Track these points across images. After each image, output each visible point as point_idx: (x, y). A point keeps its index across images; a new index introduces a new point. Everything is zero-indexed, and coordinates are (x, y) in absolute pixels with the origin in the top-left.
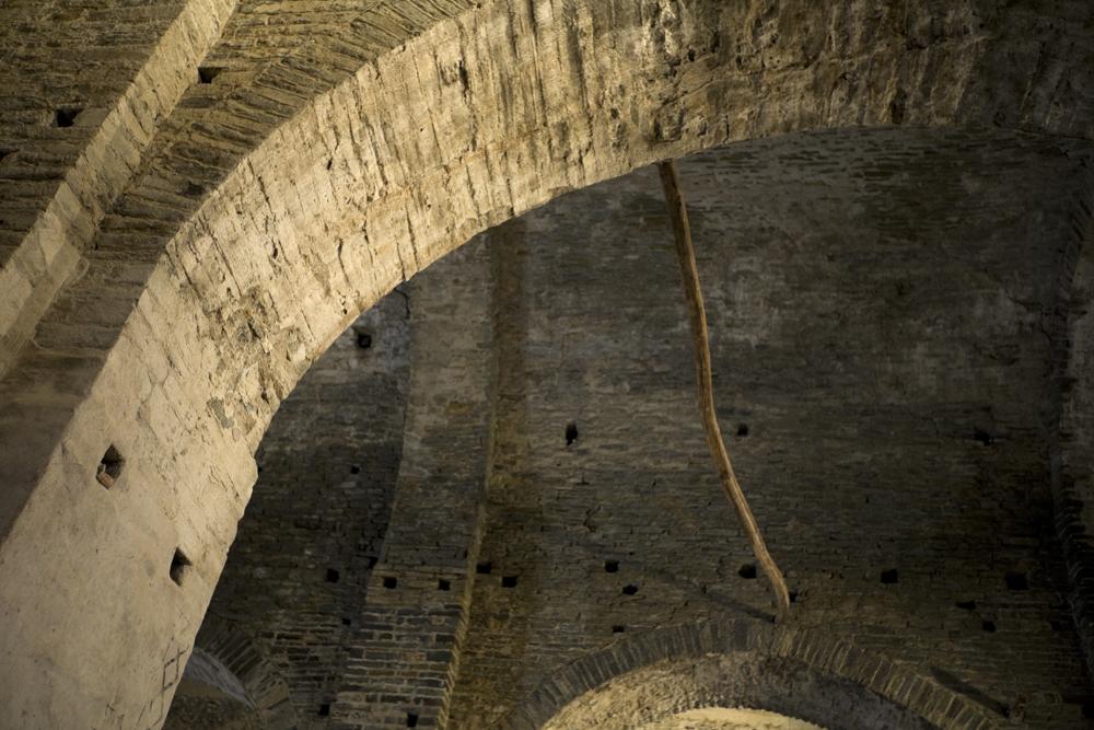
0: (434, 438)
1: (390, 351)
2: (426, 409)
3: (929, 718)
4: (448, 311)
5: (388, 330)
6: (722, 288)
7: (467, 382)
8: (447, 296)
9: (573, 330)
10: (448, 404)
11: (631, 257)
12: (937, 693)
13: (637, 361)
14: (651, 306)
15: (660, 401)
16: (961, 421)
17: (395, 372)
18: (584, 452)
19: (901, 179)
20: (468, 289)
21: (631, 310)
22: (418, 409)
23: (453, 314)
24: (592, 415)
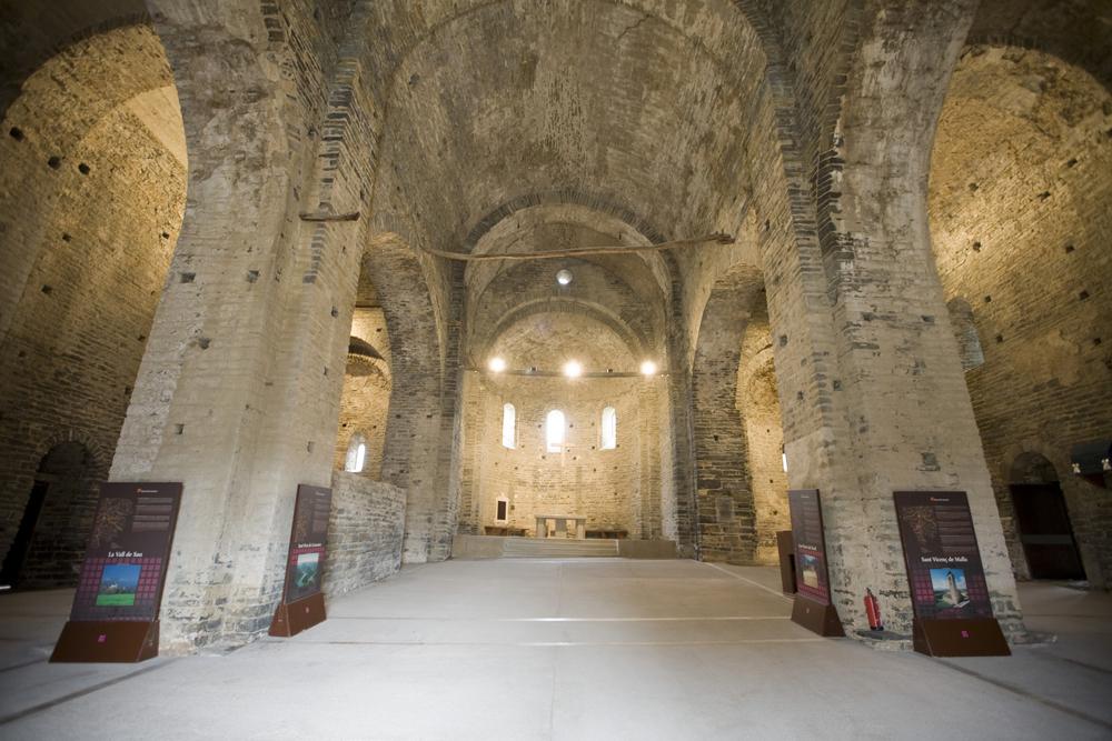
13: (455, 88)
14: (483, 81)
18: (410, 96)
19: (546, 149)
21: (479, 73)
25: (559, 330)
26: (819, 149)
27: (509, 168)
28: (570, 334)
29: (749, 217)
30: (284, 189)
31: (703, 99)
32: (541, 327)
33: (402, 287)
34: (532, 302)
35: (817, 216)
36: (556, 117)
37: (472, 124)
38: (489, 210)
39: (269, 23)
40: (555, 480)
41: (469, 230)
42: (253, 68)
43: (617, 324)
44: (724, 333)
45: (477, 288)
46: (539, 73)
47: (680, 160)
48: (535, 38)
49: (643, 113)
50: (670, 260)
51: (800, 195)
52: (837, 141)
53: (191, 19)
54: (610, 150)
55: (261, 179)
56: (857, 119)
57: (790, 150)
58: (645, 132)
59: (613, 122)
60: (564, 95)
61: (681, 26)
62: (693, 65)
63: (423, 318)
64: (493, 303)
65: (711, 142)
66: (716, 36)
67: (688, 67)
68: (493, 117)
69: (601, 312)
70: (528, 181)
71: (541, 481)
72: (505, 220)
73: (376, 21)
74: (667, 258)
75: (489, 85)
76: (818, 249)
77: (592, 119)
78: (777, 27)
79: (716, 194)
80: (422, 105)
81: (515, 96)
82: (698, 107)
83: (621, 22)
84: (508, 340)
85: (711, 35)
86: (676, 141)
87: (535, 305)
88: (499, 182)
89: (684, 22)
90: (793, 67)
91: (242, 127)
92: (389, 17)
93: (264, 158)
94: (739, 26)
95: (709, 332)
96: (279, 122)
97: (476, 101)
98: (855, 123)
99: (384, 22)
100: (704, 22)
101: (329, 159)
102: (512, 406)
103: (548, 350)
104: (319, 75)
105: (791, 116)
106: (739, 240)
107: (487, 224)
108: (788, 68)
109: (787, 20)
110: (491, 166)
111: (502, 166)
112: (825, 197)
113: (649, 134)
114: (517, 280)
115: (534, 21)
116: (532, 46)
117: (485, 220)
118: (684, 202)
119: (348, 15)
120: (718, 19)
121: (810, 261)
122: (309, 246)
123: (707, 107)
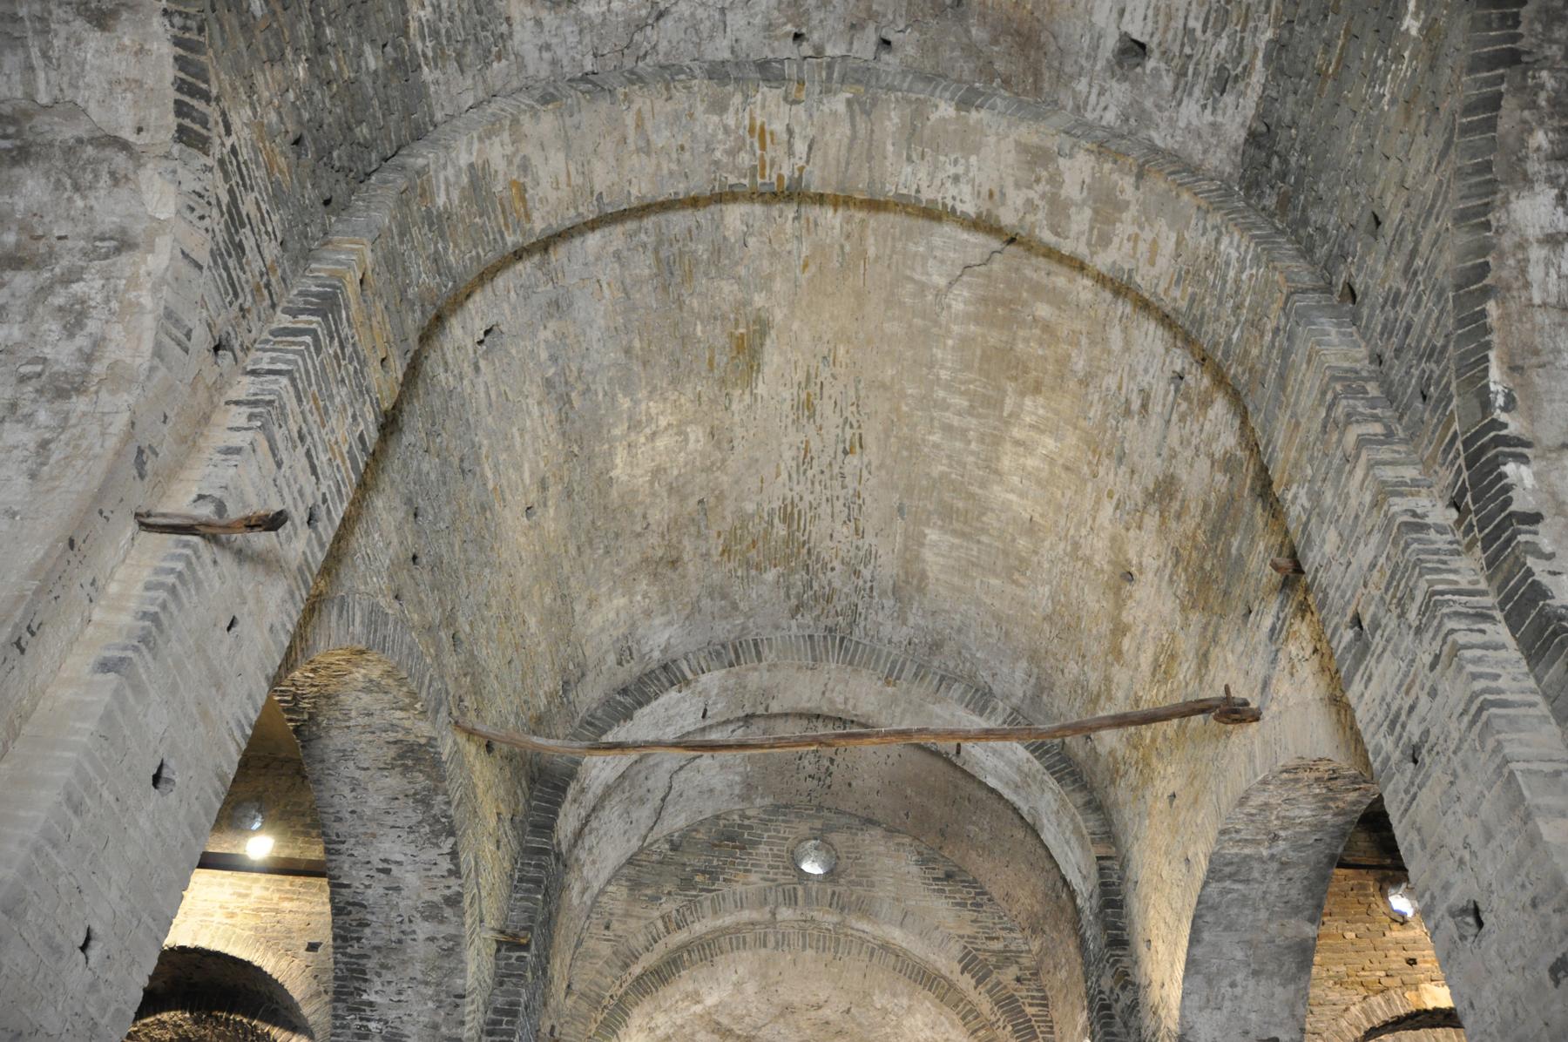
0: (478, 179)
1: (546, 37)
2: (509, 150)
4: (642, 144)
5: (576, 29)
6: (669, 425)
7: (553, 196)
8: (660, 139)
9: (605, 286)
10: (522, 180)
11: (699, 328)
13: (580, 371)
14: (645, 364)
15: (542, 415)
16: (571, 666)
17: (517, 55)
18: (477, 369)
20: (674, 167)
21: (637, 344)
22: (506, 136)
23: (638, 150)
24: (514, 351)
25: (796, 1000)
26: (1456, 426)
27: (690, 566)
28: (827, 1012)
29: (1293, 648)
30: (112, 442)
31: (1144, 406)
32: (750, 988)
33: (390, 820)
34: (727, 920)
35: (1490, 579)
36: (806, 457)
37: (611, 453)
38: (634, 668)
39: (181, 109)
41: (583, 712)
42: (123, 192)
43: (951, 986)
44: (1251, 983)
45: (588, 872)
46: (772, 358)
47: (1098, 548)
48: (766, 283)
49: (1008, 446)
50: (1088, 804)
51: (1433, 534)
52: (1500, 401)
53: (19, 94)
54: (932, 535)
55: (66, 419)
56: (1536, 352)
57: (1382, 443)
58: (1012, 491)
59: (938, 469)
60: (825, 407)
61: (1082, 250)
62: (1116, 337)
63: (432, 912)
64: (627, 914)
65: (1172, 497)
66: (1163, 262)
67: (1105, 340)
68: (661, 443)
69: (905, 952)
70: (735, 607)
72: (673, 694)
73: (425, 193)
74: (1080, 798)
75: (657, 371)
76: (1513, 652)
77: (888, 461)
78: (1295, 232)
79: (1195, 617)
80: (499, 395)
81: (713, 401)
82: (1132, 424)
83: (951, 255)
84: (660, 1019)
85: (1152, 263)
86: (1088, 505)
87: (737, 929)
88: (664, 600)
89: (1089, 244)
90: (1351, 293)
91: (60, 309)
92: (455, 195)
93: (86, 374)
94: (1213, 235)
95: (1209, 982)
96: (147, 300)
97: (625, 403)
98: (1534, 360)
99: (441, 200)
100: (1134, 239)
101: (246, 410)
104: (271, 250)
105: (1366, 380)
106: (1274, 708)
107: (627, 700)
108: (1336, 298)
109: (1315, 216)
110: (646, 560)
111: (674, 563)
112: (1500, 528)
113: (1022, 495)
114: (697, 862)
115: (767, 248)
116: (759, 300)
117: (624, 691)
118: (1117, 653)
119: (368, 175)
120: (1165, 228)
121: (1501, 683)
122: (138, 589)
123: (1155, 422)
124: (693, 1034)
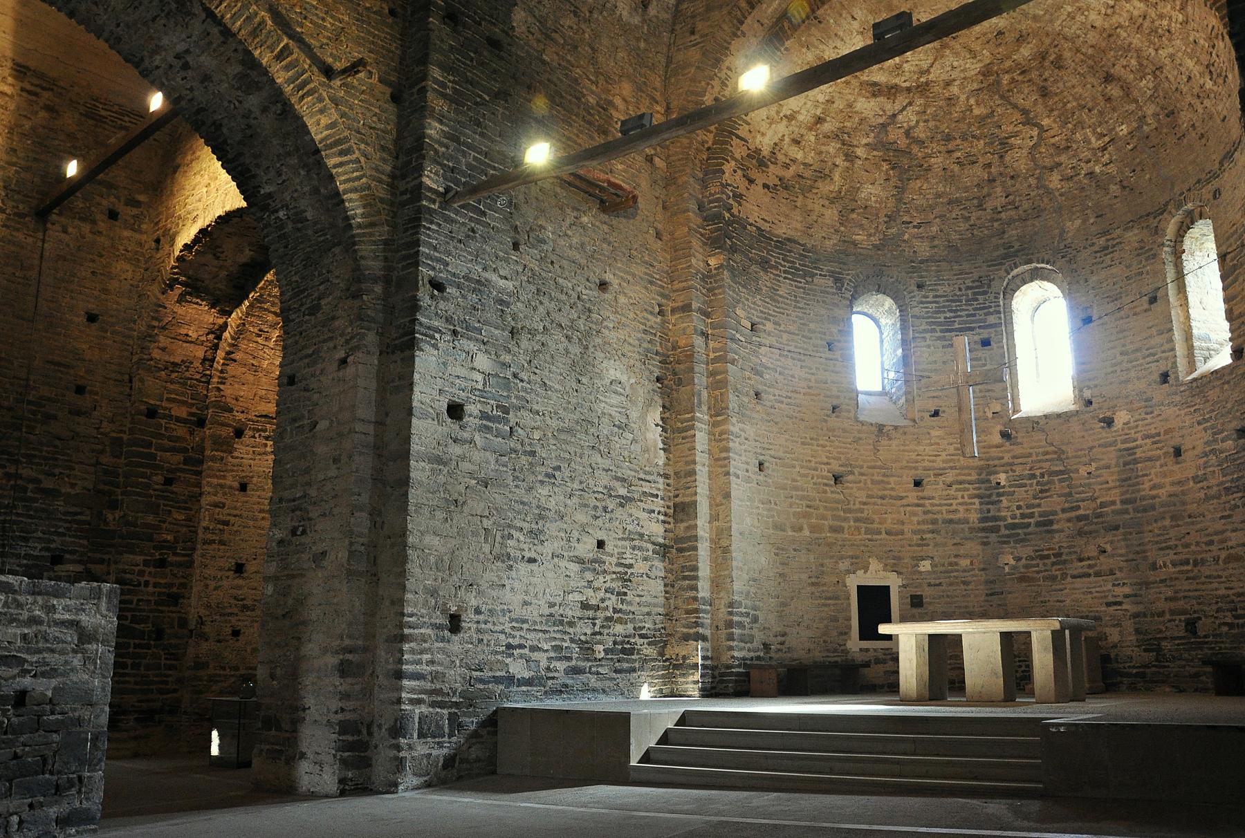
3: (257, 53)
12: (270, 32)
40: (1055, 502)
71: (1007, 509)
102: (889, 302)
103: (951, 100)
124: (850, 106)
